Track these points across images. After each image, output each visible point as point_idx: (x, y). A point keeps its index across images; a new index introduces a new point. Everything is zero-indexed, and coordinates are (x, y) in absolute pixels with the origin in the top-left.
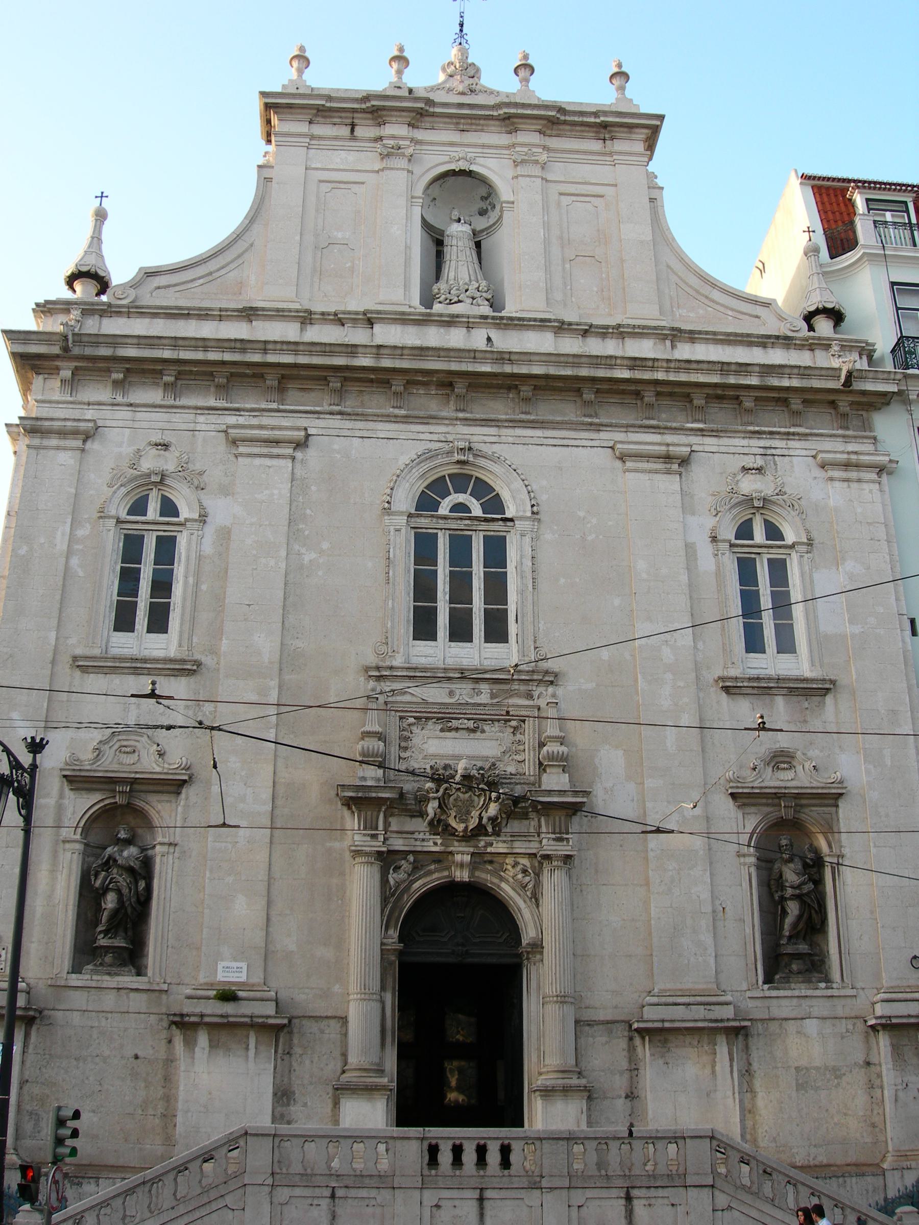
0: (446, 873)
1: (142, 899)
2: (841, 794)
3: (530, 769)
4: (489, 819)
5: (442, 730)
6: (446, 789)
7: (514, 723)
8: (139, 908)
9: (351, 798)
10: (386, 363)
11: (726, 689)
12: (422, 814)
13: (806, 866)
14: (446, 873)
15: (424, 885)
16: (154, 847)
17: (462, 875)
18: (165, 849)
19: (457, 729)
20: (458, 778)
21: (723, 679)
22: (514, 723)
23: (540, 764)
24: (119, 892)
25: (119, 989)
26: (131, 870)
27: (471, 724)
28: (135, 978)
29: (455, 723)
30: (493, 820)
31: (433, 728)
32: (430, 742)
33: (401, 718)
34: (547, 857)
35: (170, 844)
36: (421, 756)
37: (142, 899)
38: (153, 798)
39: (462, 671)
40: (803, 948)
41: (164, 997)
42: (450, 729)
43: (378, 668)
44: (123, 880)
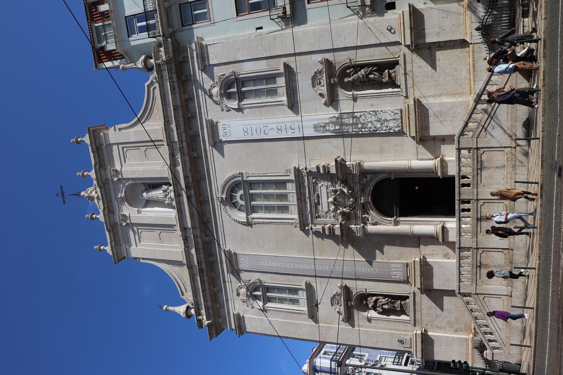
10: (198, 225)
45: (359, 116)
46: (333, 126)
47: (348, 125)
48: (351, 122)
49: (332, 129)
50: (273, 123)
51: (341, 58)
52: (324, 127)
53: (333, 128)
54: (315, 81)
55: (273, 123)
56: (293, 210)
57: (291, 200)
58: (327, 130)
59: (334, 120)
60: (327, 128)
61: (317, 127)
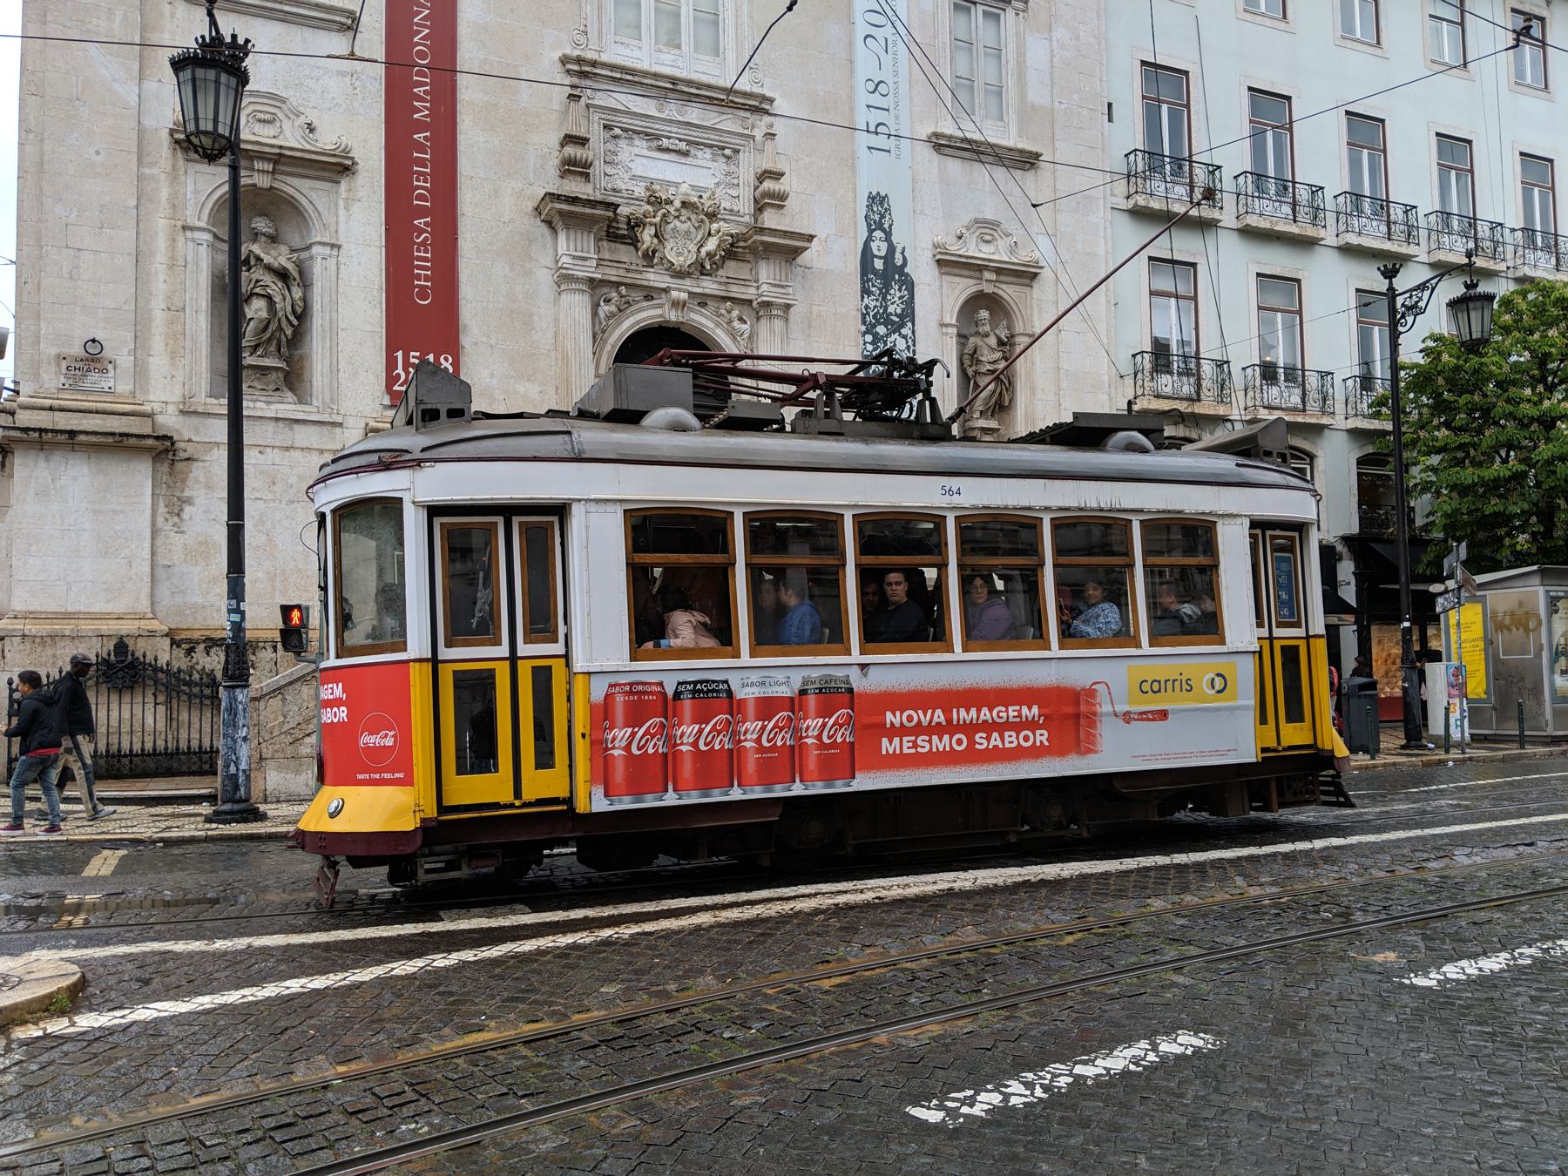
0: (659, 311)
1: (299, 310)
2: (1036, 274)
3: (746, 207)
4: (708, 254)
5: (649, 148)
6: (664, 215)
7: (727, 152)
8: (295, 322)
9: (561, 213)
11: (938, 147)
12: (634, 242)
13: (1001, 343)
14: (659, 311)
15: (638, 322)
16: (308, 248)
17: (673, 316)
18: (327, 250)
19: (668, 150)
20: (677, 204)
21: (936, 135)
22: (727, 152)
23: (756, 201)
24: (269, 298)
25: (277, 419)
26: (283, 275)
27: (683, 146)
28: (299, 407)
29: (665, 143)
30: (710, 255)
31: (641, 145)
32: (639, 160)
33: (605, 127)
34: (768, 304)
35: (333, 246)
36: (626, 176)
37: (299, 310)
38: (304, 185)
39: (674, 80)
40: (993, 424)
41: (338, 430)
42: (660, 149)
43: (579, 60)
44: (275, 287)
45: (904, 331)
46: (883, 253)
47: (884, 298)
48: (891, 309)
49: (874, 246)
50: (896, 73)
51: (1036, 312)
52: (880, 226)
53: (876, 252)
54: (987, 228)
55: (896, 73)
56: (627, 52)
57: (662, 56)
58: (871, 231)
59: (899, 261)
60: (878, 234)
61: (881, 204)
